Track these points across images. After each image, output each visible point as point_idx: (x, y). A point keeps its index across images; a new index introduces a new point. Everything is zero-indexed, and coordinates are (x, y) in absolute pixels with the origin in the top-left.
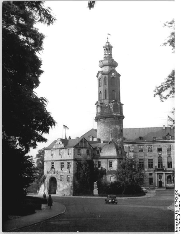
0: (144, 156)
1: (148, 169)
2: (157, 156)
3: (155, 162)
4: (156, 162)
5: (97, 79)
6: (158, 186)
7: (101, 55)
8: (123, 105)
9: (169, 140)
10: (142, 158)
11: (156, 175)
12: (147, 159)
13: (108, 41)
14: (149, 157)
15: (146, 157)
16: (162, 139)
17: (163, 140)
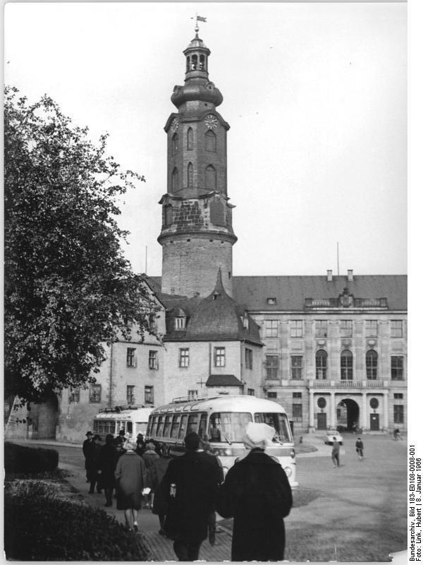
0: (281, 347)
1: (289, 382)
2: (315, 349)
3: (308, 363)
4: (311, 365)
5: (164, 137)
6: (316, 426)
7: (178, 75)
8: (235, 207)
9: (347, 307)
10: (275, 352)
11: (312, 396)
12: (289, 356)
13: (197, 35)
14: (293, 349)
15: (284, 351)
16: (329, 304)
17: (333, 307)
